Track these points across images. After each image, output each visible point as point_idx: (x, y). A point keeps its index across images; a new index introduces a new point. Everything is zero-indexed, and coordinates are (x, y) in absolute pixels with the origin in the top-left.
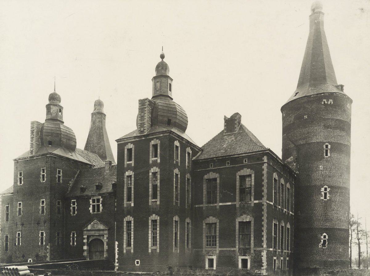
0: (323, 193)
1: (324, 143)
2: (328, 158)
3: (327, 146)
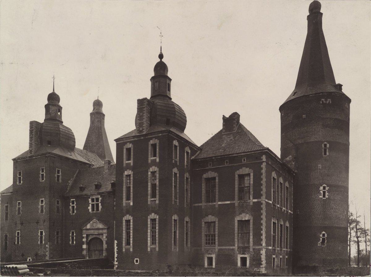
0: (322, 192)
1: (322, 142)
2: (327, 157)
3: (325, 145)
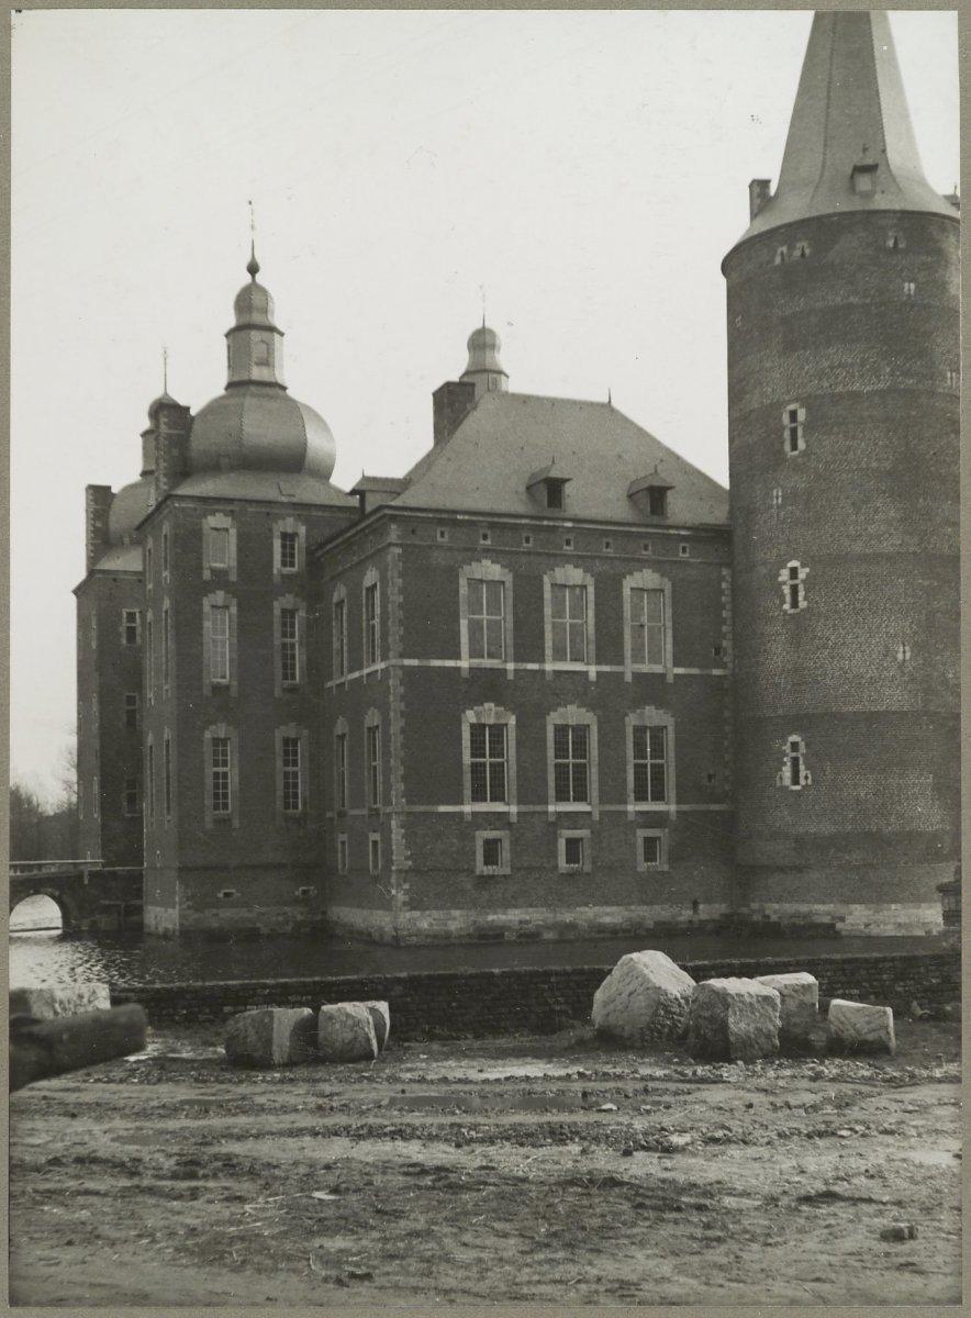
0: (787, 590)
1: (780, 405)
2: (798, 457)
3: (793, 415)
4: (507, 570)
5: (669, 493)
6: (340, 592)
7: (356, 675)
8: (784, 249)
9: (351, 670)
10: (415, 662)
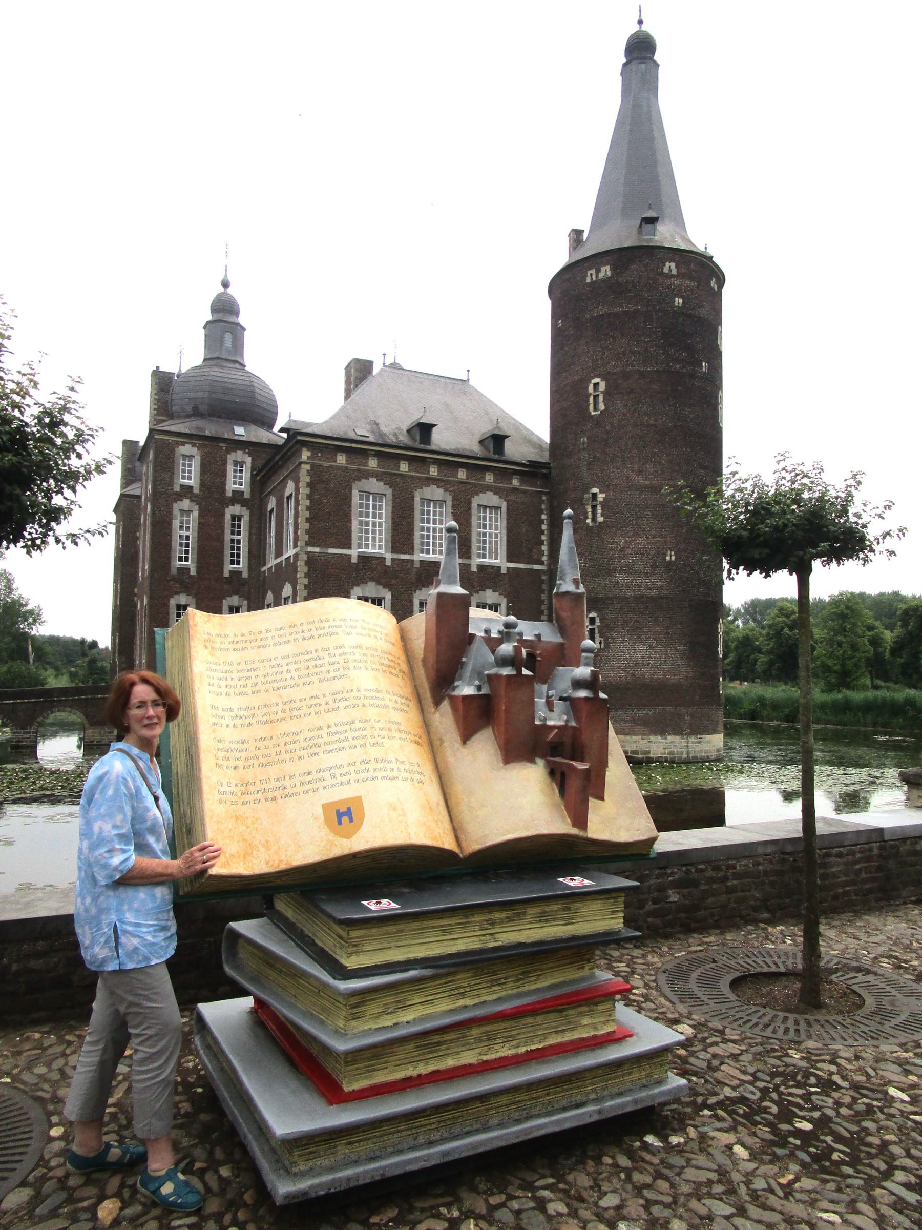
4: (388, 487)
5: (506, 440)
6: (272, 503)
7: (279, 560)
8: (593, 271)
9: (276, 557)
10: (317, 550)
